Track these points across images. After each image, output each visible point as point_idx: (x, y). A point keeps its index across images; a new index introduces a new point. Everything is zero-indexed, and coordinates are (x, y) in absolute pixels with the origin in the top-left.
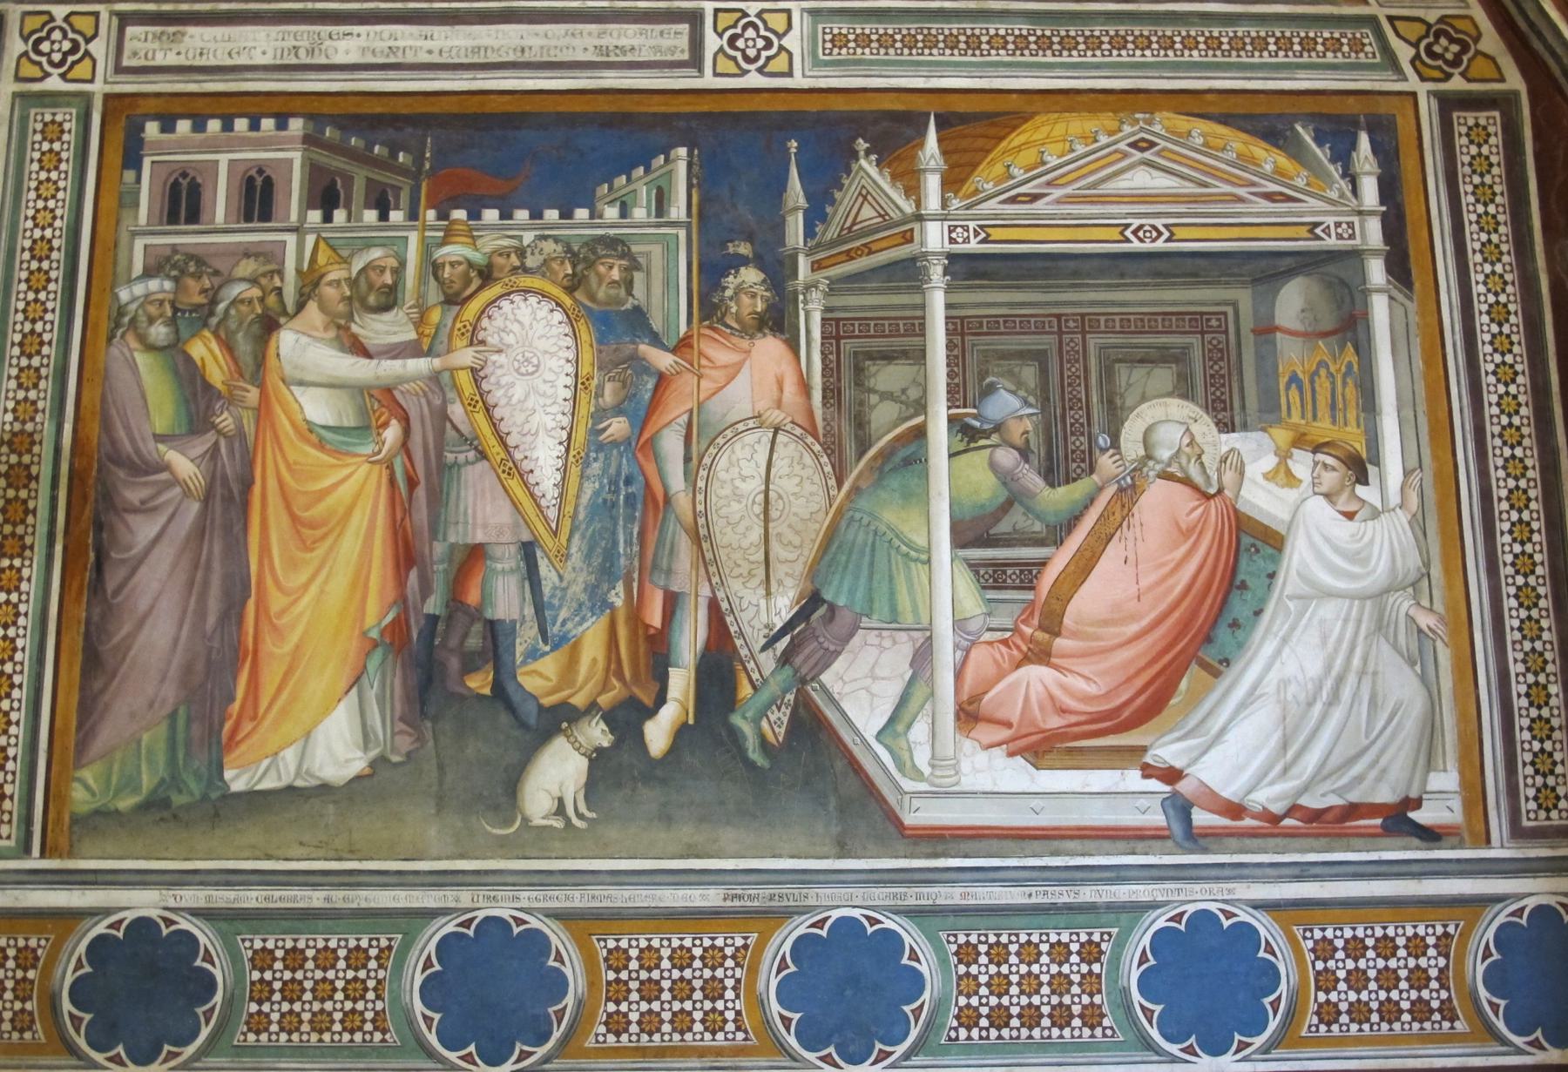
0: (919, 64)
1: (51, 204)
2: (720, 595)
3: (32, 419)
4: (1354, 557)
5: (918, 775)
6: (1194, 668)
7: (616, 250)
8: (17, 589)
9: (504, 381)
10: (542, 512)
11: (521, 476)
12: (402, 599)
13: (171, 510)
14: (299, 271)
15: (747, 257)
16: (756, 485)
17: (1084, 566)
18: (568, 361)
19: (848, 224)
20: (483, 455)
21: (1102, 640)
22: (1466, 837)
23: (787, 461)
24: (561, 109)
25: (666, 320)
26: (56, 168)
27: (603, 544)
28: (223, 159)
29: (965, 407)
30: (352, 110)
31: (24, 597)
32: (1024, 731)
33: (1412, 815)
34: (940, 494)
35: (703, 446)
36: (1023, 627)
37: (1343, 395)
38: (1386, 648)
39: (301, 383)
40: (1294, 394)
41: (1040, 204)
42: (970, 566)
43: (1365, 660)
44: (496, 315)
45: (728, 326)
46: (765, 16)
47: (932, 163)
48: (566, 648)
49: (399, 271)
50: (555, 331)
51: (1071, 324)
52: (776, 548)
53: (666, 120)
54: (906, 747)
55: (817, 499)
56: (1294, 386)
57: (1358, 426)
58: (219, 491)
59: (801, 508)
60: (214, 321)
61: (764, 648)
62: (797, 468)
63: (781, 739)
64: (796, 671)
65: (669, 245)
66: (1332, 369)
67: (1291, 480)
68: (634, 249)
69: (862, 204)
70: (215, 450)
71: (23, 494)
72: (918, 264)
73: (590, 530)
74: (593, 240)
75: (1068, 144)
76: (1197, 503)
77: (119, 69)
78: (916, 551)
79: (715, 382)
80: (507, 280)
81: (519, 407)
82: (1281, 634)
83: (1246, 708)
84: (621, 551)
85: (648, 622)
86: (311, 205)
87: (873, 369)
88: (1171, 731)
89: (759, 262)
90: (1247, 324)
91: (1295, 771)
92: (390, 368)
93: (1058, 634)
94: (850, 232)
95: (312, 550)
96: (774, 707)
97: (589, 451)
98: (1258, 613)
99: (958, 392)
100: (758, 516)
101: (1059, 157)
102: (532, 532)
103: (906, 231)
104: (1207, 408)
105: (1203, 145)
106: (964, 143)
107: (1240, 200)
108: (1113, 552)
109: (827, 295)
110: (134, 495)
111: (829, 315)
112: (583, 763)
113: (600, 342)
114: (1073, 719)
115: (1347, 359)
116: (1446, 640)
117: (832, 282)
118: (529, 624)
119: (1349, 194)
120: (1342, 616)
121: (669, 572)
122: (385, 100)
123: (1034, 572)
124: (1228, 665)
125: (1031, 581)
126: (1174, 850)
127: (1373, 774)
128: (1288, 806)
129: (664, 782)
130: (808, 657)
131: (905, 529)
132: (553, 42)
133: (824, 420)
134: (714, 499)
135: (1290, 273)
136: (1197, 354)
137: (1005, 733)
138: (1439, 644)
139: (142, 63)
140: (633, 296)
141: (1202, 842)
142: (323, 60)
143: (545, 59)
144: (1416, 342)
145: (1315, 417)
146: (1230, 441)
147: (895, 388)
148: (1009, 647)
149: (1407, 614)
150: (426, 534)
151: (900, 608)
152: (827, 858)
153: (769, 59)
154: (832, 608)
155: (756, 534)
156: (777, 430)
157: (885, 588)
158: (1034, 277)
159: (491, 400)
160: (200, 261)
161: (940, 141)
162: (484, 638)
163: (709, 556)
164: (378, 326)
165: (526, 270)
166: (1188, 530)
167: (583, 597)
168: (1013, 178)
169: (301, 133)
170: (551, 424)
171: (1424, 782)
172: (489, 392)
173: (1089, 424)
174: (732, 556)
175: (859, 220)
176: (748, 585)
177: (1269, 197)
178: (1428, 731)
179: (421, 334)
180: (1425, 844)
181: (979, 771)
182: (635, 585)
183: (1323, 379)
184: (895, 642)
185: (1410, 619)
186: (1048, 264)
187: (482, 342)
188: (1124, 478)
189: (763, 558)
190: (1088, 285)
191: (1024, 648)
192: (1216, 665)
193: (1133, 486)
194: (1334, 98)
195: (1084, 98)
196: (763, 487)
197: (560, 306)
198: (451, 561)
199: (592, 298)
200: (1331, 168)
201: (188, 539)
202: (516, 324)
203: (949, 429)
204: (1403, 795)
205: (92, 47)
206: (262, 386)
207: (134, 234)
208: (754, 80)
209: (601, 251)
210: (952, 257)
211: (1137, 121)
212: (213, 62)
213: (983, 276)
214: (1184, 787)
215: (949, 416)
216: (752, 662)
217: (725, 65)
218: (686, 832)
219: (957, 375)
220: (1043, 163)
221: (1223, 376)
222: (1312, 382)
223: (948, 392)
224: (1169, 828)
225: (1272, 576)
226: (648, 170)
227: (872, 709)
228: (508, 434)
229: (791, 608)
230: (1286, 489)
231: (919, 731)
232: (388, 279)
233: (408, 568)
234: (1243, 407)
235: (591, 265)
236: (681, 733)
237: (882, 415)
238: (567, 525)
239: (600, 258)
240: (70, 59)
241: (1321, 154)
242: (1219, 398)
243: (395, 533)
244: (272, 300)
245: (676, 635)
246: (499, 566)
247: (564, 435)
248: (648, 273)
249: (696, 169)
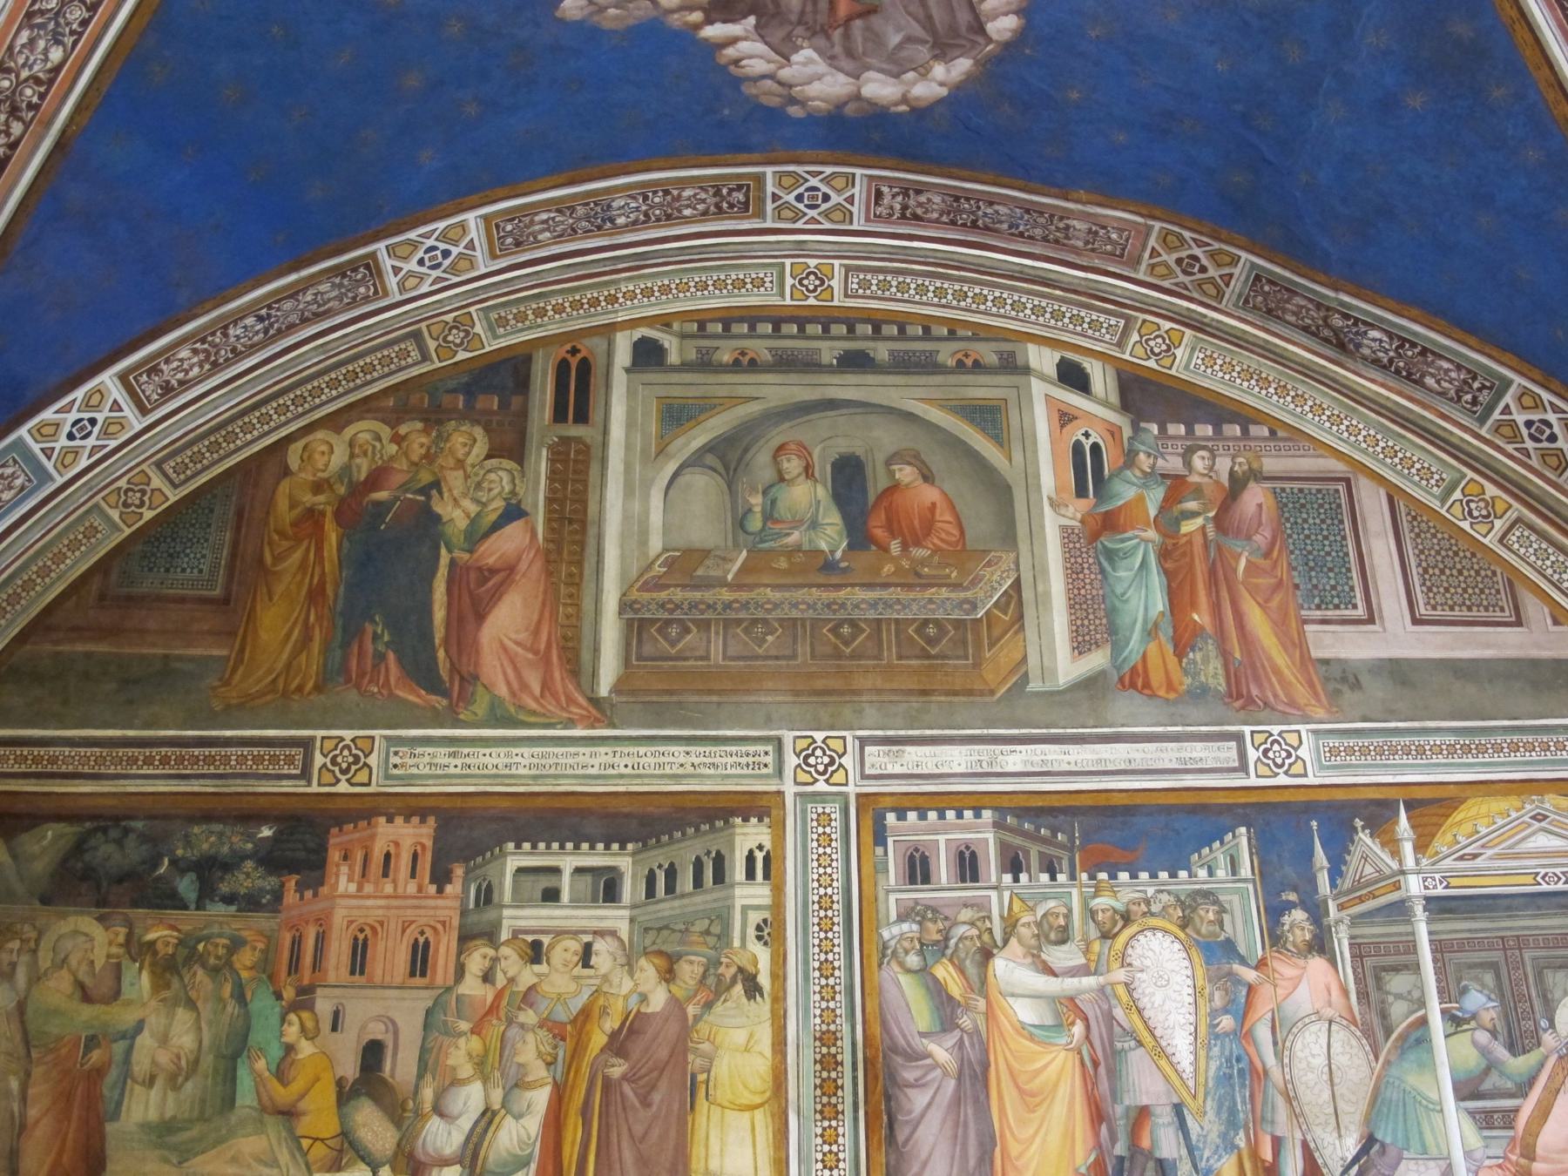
0: (1386, 766)
1: (829, 870)
2: (1309, 1138)
3: (834, 1022)
8: (836, 1142)
12: (1098, 1145)
13: (936, 1085)
14: (1002, 917)
16: (1321, 1061)
17: (1543, 1112)
20: (1140, 1044)
23: (1340, 1043)
24: (1160, 802)
25: (1248, 948)
26: (829, 845)
28: (942, 839)
30: (1022, 804)
31: (841, 1148)
39: (1013, 995)
42: (1469, 1113)
46: (1284, 735)
49: (1068, 916)
53: (1229, 808)
58: (967, 1071)
60: (949, 952)
62: (1348, 1048)
65: (1243, 895)
70: (961, 1041)
71: (833, 1075)
77: (864, 777)
86: (1004, 871)
87: (1387, 978)
89: (1303, 905)
92: (1070, 984)
93: (1533, 1159)
95: (1034, 1111)
106: (1426, 819)
109: (1350, 927)
110: (909, 1075)
113: (1207, 963)
118: (1184, 1161)
121: (1273, 1122)
122: (1044, 797)
132: (1149, 756)
139: (879, 772)
142: (999, 770)
143: (1145, 767)
150: (1109, 1099)
153: (1290, 765)
154: (1383, 1146)
155: (1327, 1095)
156: (1330, 1022)
159: (1141, 1005)
160: (935, 910)
161: (1409, 819)
163: (1298, 1110)
164: (1059, 954)
165: (1153, 915)
167: (1218, 1141)
169: (991, 820)
170: (1184, 1021)
179: (1089, 960)
184: (1427, 1169)
186: (1490, 902)
187: (1130, 965)
190: (1517, 916)
195: (1497, 786)
198: (1127, 1117)
199: (1198, 933)
201: (949, 1106)
205: (843, 761)
206: (986, 997)
207: (888, 892)
208: (1283, 780)
209: (1200, 901)
210: (1428, 899)
211: (1534, 801)
212: (926, 771)
213: (1450, 911)
217: (1263, 770)
220: (1478, 832)
226: (1222, 843)
232: (1062, 921)
233: (1100, 1124)
235: (1194, 910)
237: (1397, 1009)
240: (830, 769)
243: (1089, 1099)
244: (986, 937)
245: (1283, 1166)
246: (1160, 1121)
247: (1192, 1029)
248: (1232, 916)
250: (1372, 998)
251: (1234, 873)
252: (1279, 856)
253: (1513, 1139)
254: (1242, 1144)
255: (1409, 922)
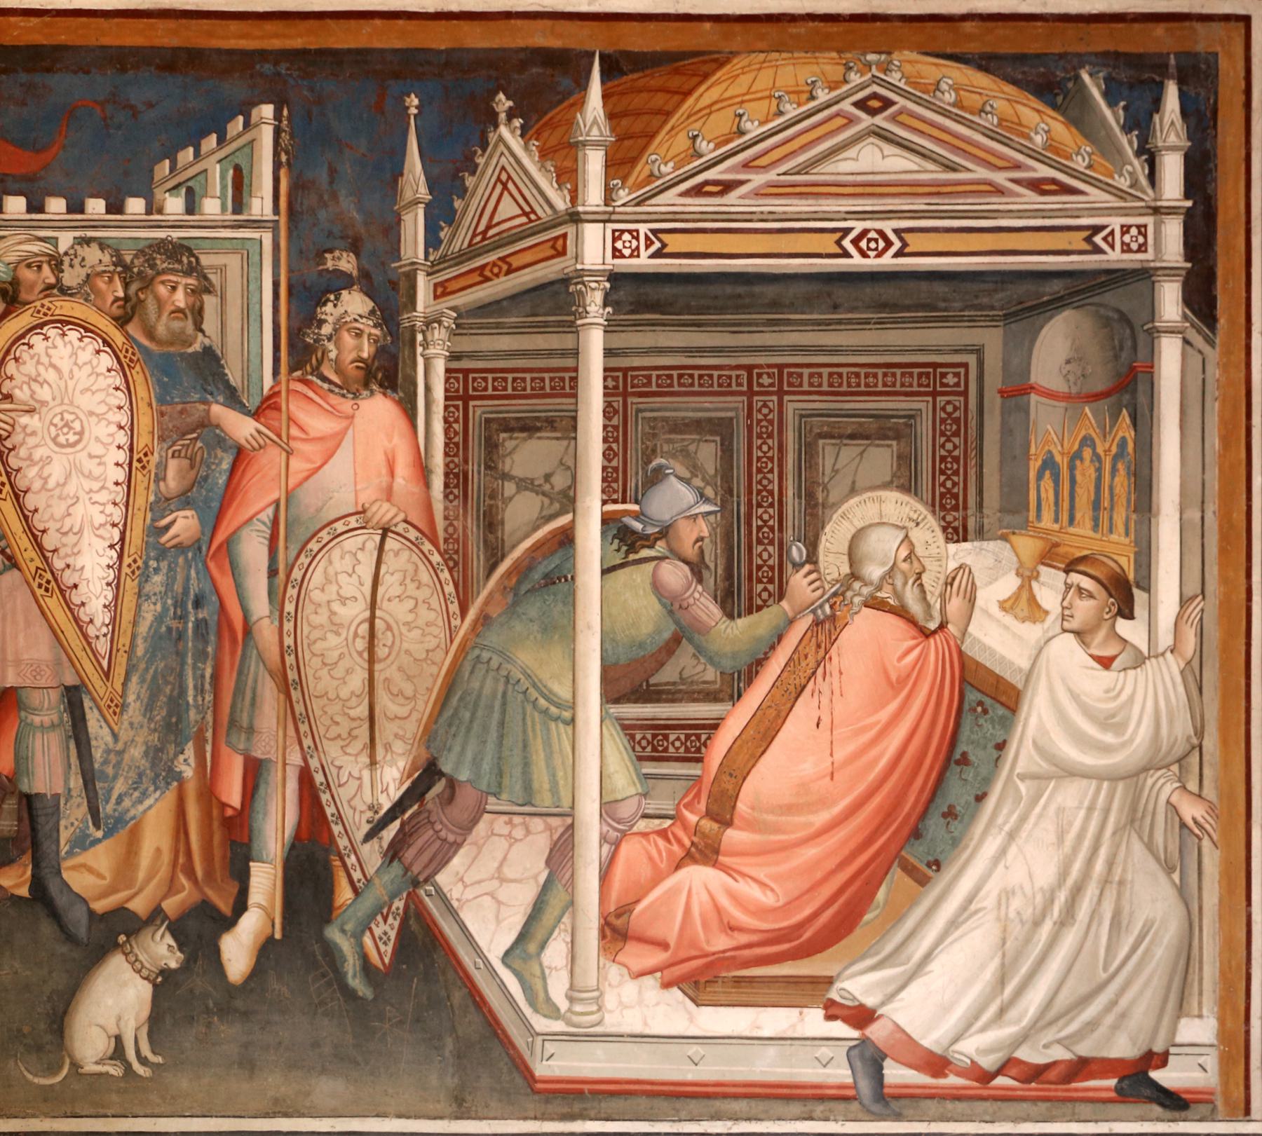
2: (314, 763)
4: (1109, 722)
5: (553, 1012)
6: (896, 873)
7: (180, 262)
9: (37, 454)
10: (89, 644)
11: (61, 591)
15: (350, 276)
16: (356, 611)
18: (121, 428)
19: (481, 228)
20: (13, 563)
21: (784, 832)
22: (1219, 1103)
23: (398, 576)
24: (106, 41)
25: (247, 374)
27: (168, 690)
29: (624, 502)
32: (683, 954)
33: (1154, 1075)
34: (589, 627)
35: (293, 554)
36: (687, 814)
37: (1111, 488)
38: (1137, 847)
40: (1047, 483)
41: (732, 197)
42: (625, 728)
43: (1110, 864)
44: (25, 356)
45: (325, 379)
47: (595, 131)
48: (123, 833)
50: (103, 382)
51: (766, 380)
52: (383, 699)
53: (244, 61)
54: (538, 973)
55: (435, 631)
56: (1047, 473)
57: (1127, 534)
59: (413, 642)
61: (369, 837)
62: (411, 586)
63: (387, 960)
64: (407, 869)
66: (1100, 450)
67: (1035, 612)
68: (205, 260)
69: (501, 195)
72: (572, 289)
73: (151, 671)
74: (150, 246)
75: (774, 102)
76: (912, 643)
78: (558, 706)
79: (309, 460)
80: (38, 304)
81: (57, 492)
82: (1007, 828)
83: (957, 928)
84: (190, 699)
85: (224, 799)
87: (510, 445)
88: (863, 957)
89: (365, 282)
90: (994, 380)
91: (1013, 1014)
93: (729, 824)
94: (484, 239)
96: (379, 918)
97: (149, 558)
98: (980, 798)
99: (616, 480)
100: (360, 654)
101: (762, 123)
102: (77, 672)
103: (556, 238)
104: (933, 505)
105: (954, 105)
107: (999, 191)
108: (804, 711)
109: (453, 334)
111: (455, 365)
112: (146, 990)
113: (161, 401)
114: (744, 939)
115: (1120, 434)
116: (1215, 837)
117: (460, 316)
119: (1144, 181)
120: (1086, 804)
121: (251, 730)
123: (703, 737)
124: (938, 870)
125: (698, 750)
126: (860, 1116)
127: (1109, 1019)
128: (1004, 1059)
129: (246, 1015)
130: (421, 851)
131: (544, 674)
133: (446, 518)
134: (306, 629)
135: (1057, 304)
136: (925, 428)
137: (659, 957)
138: (1206, 843)
140: (202, 331)
141: (895, 1105)
144: (1214, 408)
145: (1072, 520)
146: (960, 553)
147: (537, 473)
148: (668, 841)
149: (1168, 802)
151: (536, 785)
152: (441, 1118)
154: (452, 784)
155: (358, 680)
156: (385, 531)
157: (516, 759)
158: (722, 310)
159: (21, 483)
161: (605, 97)
162: (20, 820)
163: (299, 708)
165: (64, 291)
166: (898, 681)
167: (145, 764)
168: (701, 156)
170: (99, 519)
171: (1173, 1031)
172: (18, 471)
173: (781, 529)
174: (330, 710)
175: (496, 220)
176: (349, 750)
177: (1037, 186)
178: (1182, 962)
180: (1168, 1114)
181: (626, 1007)
182: (209, 748)
183: (1087, 463)
184: (528, 832)
185: (1172, 808)
186: (740, 290)
188: (821, 606)
189: (366, 713)
190: (788, 322)
191: (687, 843)
192: (924, 868)
193: (833, 618)
194: (1136, 26)
196: (367, 614)
197: (110, 346)
199: (150, 334)
200: (1124, 140)
202: (51, 370)
203: (603, 533)
204: (1144, 1049)
209: (161, 265)
210: (616, 278)
211: (869, 66)
214: (876, 1032)
215: (603, 514)
216: (353, 857)
218: (274, 1082)
219: (616, 455)
220: (741, 133)
221: (956, 459)
222: (1072, 468)
223: (604, 480)
224: (855, 1086)
225: (1001, 746)
227: (498, 920)
228: (44, 531)
229: (402, 783)
230: (1027, 624)
231: (555, 953)
234: (980, 505)
235: (148, 284)
236: (267, 950)
238: (122, 660)
239: (159, 274)
241: (1111, 116)
242: (949, 491)
246: (37, 720)
249: (285, 137)
250: (473, 487)
251: (239, 205)
252: (333, 172)
253: (698, 780)
254: (188, 772)
255: (571, 328)
